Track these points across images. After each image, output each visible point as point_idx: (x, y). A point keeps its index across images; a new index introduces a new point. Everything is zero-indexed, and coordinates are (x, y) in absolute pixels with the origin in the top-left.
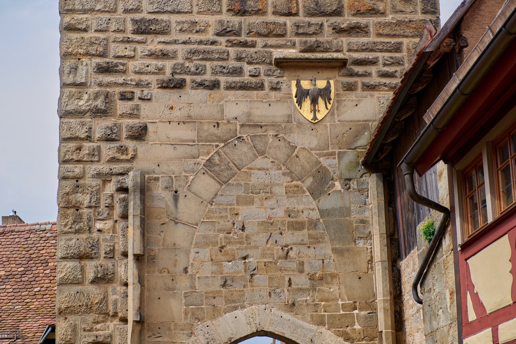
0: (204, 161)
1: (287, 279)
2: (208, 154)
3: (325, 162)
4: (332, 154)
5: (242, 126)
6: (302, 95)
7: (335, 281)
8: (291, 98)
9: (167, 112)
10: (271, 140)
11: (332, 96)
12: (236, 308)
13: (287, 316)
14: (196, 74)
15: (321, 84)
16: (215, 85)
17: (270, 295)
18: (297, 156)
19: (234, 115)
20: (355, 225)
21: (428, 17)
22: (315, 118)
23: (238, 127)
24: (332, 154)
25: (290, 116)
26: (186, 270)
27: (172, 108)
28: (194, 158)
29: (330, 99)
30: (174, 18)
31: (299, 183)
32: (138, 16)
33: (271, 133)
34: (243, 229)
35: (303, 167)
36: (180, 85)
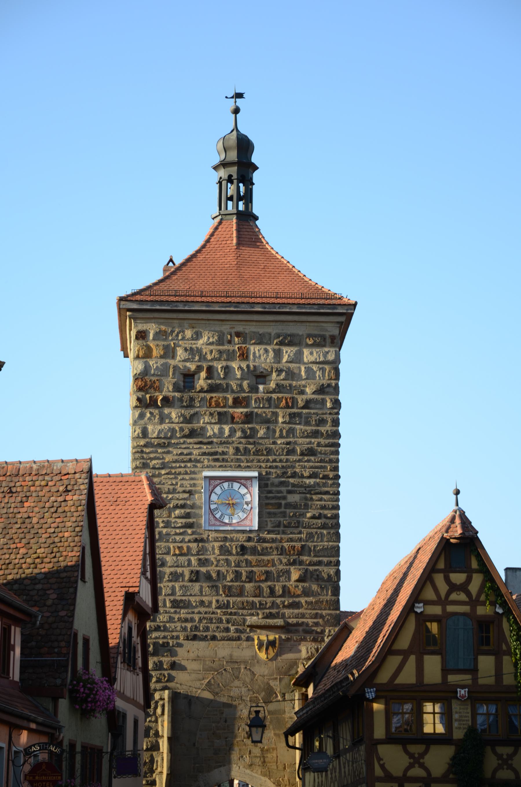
0: (206, 683)
1: (249, 750)
2: (208, 678)
3: (272, 683)
4: (276, 679)
5: (227, 662)
6: (260, 645)
7: (275, 752)
8: (254, 646)
9: (186, 654)
10: (242, 670)
11: (277, 645)
12: (220, 766)
13: (248, 771)
14: (203, 632)
15: (271, 638)
16: (214, 638)
17: (239, 759)
18: (257, 680)
19: (223, 656)
20: (286, 720)
21: (333, 598)
22: (267, 658)
23: (225, 663)
24: (276, 679)
25: (253, 656)
26: (194, 745)
27: (188, 652)
28: (200, 680)
29: (275, 647)
30: (192, 599)
31: (258, 695)
32: (172, 598)
33: (242, 667)
34: (226, 721)
35: (260, 686)
36: (195, 638)
